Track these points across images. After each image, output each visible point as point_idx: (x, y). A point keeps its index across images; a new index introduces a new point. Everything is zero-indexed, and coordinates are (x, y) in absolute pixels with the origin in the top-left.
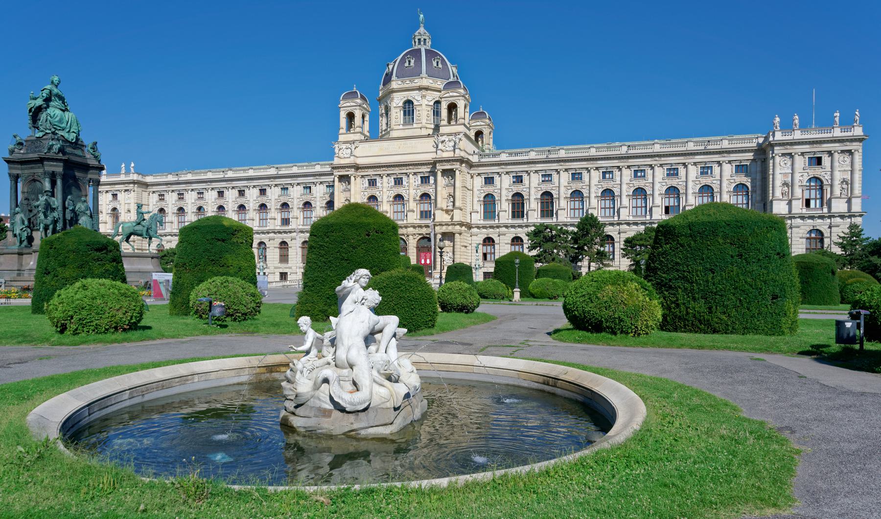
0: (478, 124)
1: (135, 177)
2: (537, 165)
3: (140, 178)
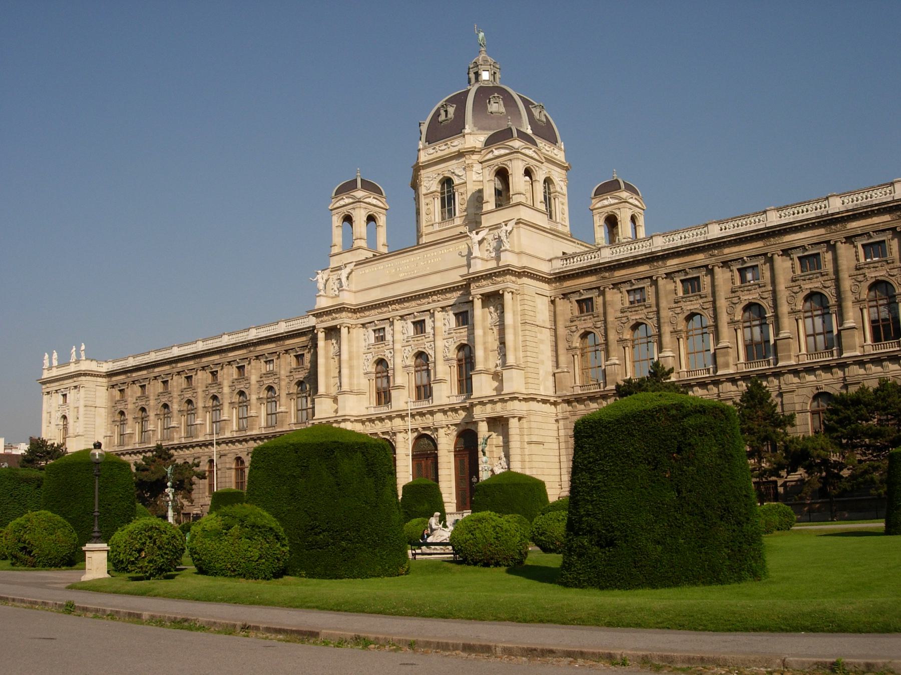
0: (606, 202)
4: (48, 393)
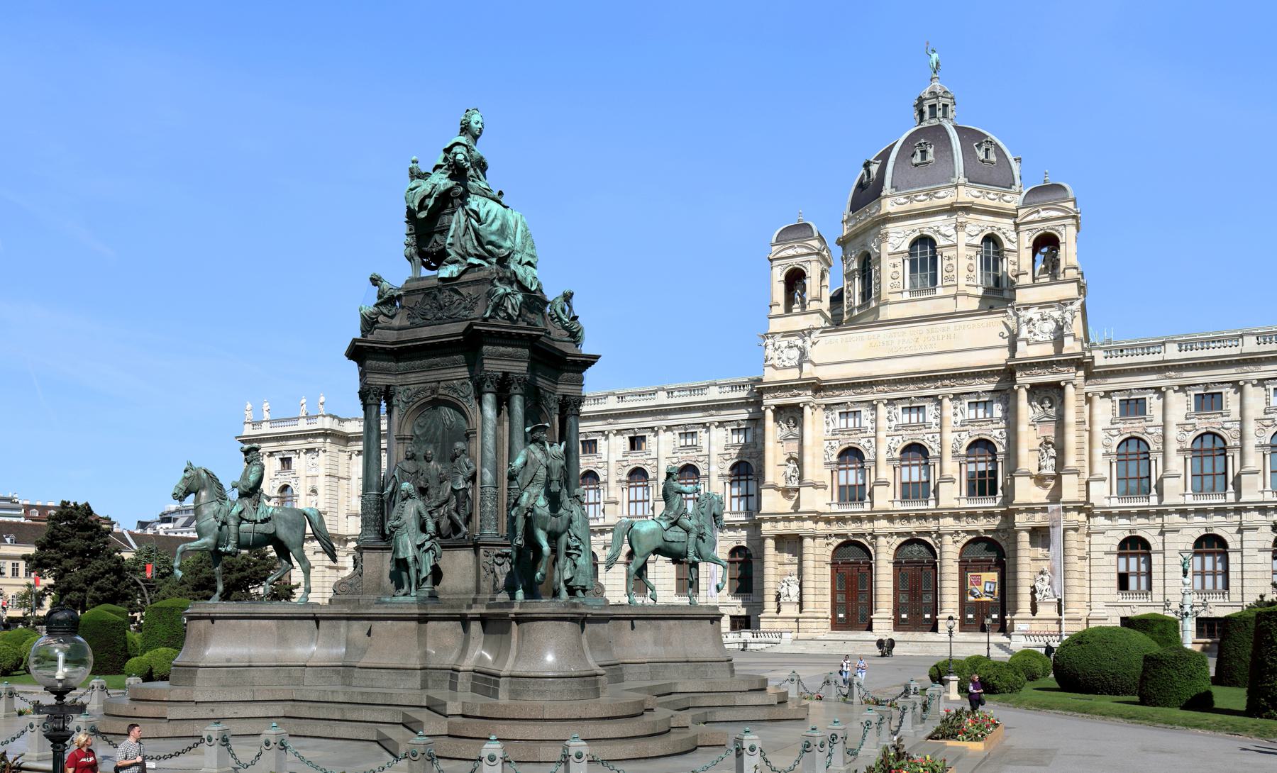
1: (327, 424)
3: (334, 425)
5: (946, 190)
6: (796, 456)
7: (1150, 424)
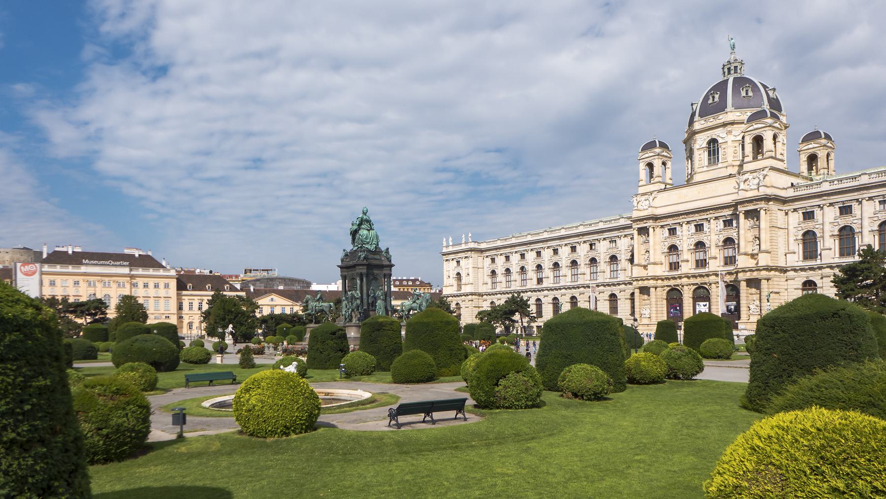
1: (472, 245)
2: (871, 191)
4: (447, 260)
5: (722, 115)
6: (758, 236)
7: (816, 223)
